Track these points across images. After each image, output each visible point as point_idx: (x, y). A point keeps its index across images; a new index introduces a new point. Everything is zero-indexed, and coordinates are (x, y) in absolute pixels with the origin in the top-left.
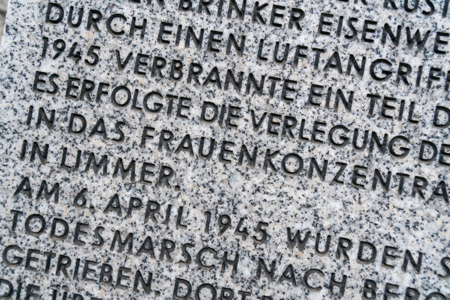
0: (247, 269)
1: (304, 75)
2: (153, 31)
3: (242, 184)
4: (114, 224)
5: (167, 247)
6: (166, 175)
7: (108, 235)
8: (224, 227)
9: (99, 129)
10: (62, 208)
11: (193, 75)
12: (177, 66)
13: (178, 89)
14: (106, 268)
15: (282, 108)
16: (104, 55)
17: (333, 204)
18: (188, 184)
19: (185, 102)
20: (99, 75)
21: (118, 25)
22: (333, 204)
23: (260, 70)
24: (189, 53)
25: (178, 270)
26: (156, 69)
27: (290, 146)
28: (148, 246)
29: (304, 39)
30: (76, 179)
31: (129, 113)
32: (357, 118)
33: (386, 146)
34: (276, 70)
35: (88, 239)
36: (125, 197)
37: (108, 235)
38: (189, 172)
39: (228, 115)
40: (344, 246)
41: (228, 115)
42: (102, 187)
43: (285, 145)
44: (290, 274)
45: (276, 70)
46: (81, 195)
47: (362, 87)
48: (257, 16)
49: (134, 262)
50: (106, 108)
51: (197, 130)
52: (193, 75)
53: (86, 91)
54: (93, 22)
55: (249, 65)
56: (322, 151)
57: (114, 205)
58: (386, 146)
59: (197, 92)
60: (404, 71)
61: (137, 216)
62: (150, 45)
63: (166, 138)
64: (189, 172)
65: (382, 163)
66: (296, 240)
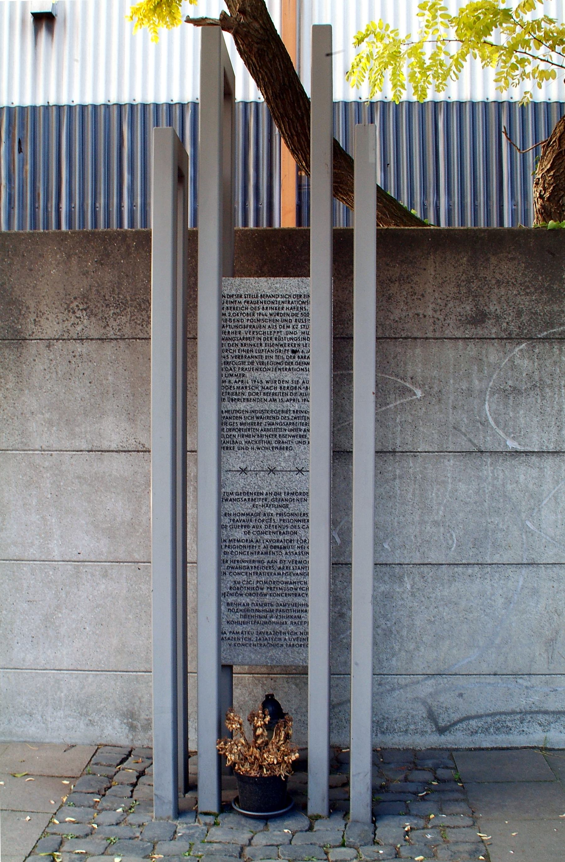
0: (260, 389)
1: (264, 354)
2: (237, 351)
3: (256, 374)
4: (236, 385)
5: (246, 387)
6: (243, 375)
7: (235, 387)
8: (255, 381)
9: (231, 369)
10: (227, 384)
11: (245, 358)
12: (242, 356)
13: (243, 360)
14: (236, 393)
15: (261, 360)
16: (229, 356)
17: (272, 375)
18: (248, 376)
19: (245, 362)
20: (229, 360)
21: (231, 351)
22: (272, 375)
23: (256, 355)
24: (244, 354)
25: (248, 391)
26: (239, 358)
27: (263, 367)
28: (243, 388)
29: (263, 348)
30: (228, 378)
31: (235, 366)
32: (274, 360)
33: (279, 364)
34: (259, 354)
35: (232, 389)
36: (237, 380)
37: (235, 387)
38: (247, 374)
39: (252, 363)
40: (275, 381)
41: (252, 363)
42: (233, 379)
43: (262, 366)
44: (267, 388)
45: (259, 354)
46: (230, 381)
47: (274, 354)
48: (254, 346)
49: (241, 391)
50: (232, 365)
51: (247, 367)
52: (245, 358)
53: (227, 363)
54: (226, 352)
55: (255, 354)
56: (269, 366)
57: (236, 382)
58: (279, 364)
59: (247, 360)
60: (280, 351)
61: (240, 383)
62: (237, 354)
63: (242, 369)
64: (247, 374)
65: (279, 366)
66: (267, 382)
